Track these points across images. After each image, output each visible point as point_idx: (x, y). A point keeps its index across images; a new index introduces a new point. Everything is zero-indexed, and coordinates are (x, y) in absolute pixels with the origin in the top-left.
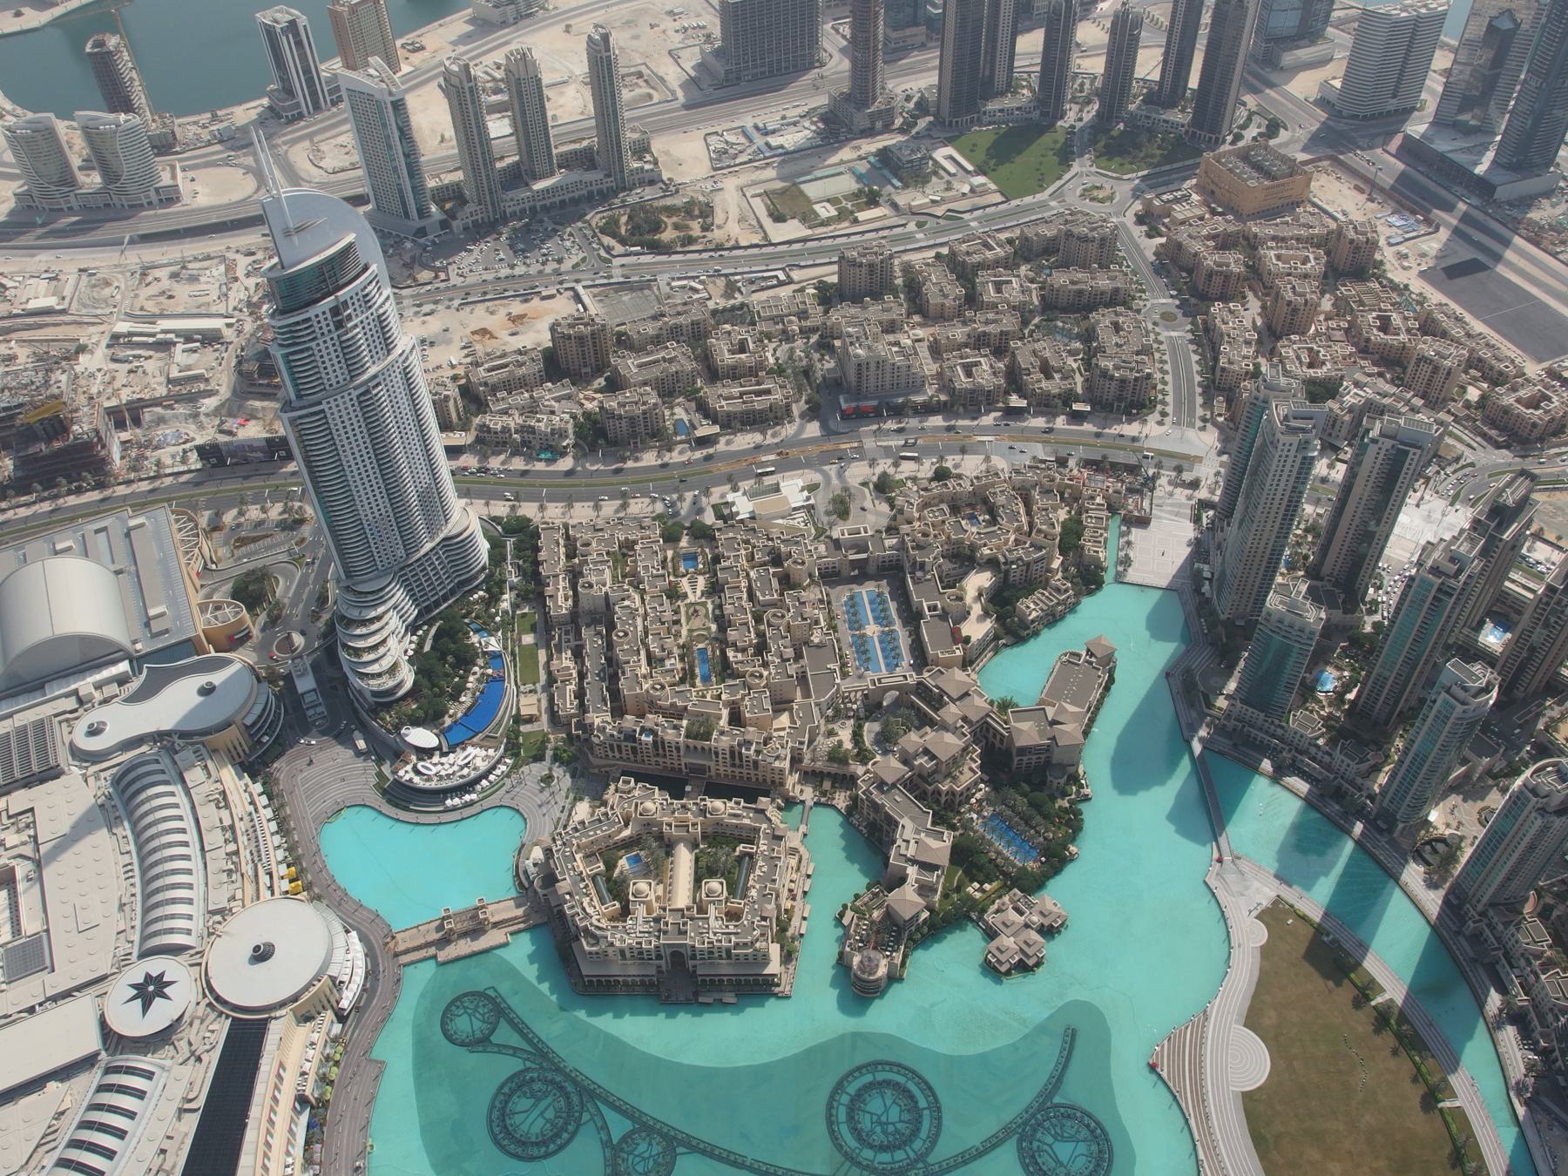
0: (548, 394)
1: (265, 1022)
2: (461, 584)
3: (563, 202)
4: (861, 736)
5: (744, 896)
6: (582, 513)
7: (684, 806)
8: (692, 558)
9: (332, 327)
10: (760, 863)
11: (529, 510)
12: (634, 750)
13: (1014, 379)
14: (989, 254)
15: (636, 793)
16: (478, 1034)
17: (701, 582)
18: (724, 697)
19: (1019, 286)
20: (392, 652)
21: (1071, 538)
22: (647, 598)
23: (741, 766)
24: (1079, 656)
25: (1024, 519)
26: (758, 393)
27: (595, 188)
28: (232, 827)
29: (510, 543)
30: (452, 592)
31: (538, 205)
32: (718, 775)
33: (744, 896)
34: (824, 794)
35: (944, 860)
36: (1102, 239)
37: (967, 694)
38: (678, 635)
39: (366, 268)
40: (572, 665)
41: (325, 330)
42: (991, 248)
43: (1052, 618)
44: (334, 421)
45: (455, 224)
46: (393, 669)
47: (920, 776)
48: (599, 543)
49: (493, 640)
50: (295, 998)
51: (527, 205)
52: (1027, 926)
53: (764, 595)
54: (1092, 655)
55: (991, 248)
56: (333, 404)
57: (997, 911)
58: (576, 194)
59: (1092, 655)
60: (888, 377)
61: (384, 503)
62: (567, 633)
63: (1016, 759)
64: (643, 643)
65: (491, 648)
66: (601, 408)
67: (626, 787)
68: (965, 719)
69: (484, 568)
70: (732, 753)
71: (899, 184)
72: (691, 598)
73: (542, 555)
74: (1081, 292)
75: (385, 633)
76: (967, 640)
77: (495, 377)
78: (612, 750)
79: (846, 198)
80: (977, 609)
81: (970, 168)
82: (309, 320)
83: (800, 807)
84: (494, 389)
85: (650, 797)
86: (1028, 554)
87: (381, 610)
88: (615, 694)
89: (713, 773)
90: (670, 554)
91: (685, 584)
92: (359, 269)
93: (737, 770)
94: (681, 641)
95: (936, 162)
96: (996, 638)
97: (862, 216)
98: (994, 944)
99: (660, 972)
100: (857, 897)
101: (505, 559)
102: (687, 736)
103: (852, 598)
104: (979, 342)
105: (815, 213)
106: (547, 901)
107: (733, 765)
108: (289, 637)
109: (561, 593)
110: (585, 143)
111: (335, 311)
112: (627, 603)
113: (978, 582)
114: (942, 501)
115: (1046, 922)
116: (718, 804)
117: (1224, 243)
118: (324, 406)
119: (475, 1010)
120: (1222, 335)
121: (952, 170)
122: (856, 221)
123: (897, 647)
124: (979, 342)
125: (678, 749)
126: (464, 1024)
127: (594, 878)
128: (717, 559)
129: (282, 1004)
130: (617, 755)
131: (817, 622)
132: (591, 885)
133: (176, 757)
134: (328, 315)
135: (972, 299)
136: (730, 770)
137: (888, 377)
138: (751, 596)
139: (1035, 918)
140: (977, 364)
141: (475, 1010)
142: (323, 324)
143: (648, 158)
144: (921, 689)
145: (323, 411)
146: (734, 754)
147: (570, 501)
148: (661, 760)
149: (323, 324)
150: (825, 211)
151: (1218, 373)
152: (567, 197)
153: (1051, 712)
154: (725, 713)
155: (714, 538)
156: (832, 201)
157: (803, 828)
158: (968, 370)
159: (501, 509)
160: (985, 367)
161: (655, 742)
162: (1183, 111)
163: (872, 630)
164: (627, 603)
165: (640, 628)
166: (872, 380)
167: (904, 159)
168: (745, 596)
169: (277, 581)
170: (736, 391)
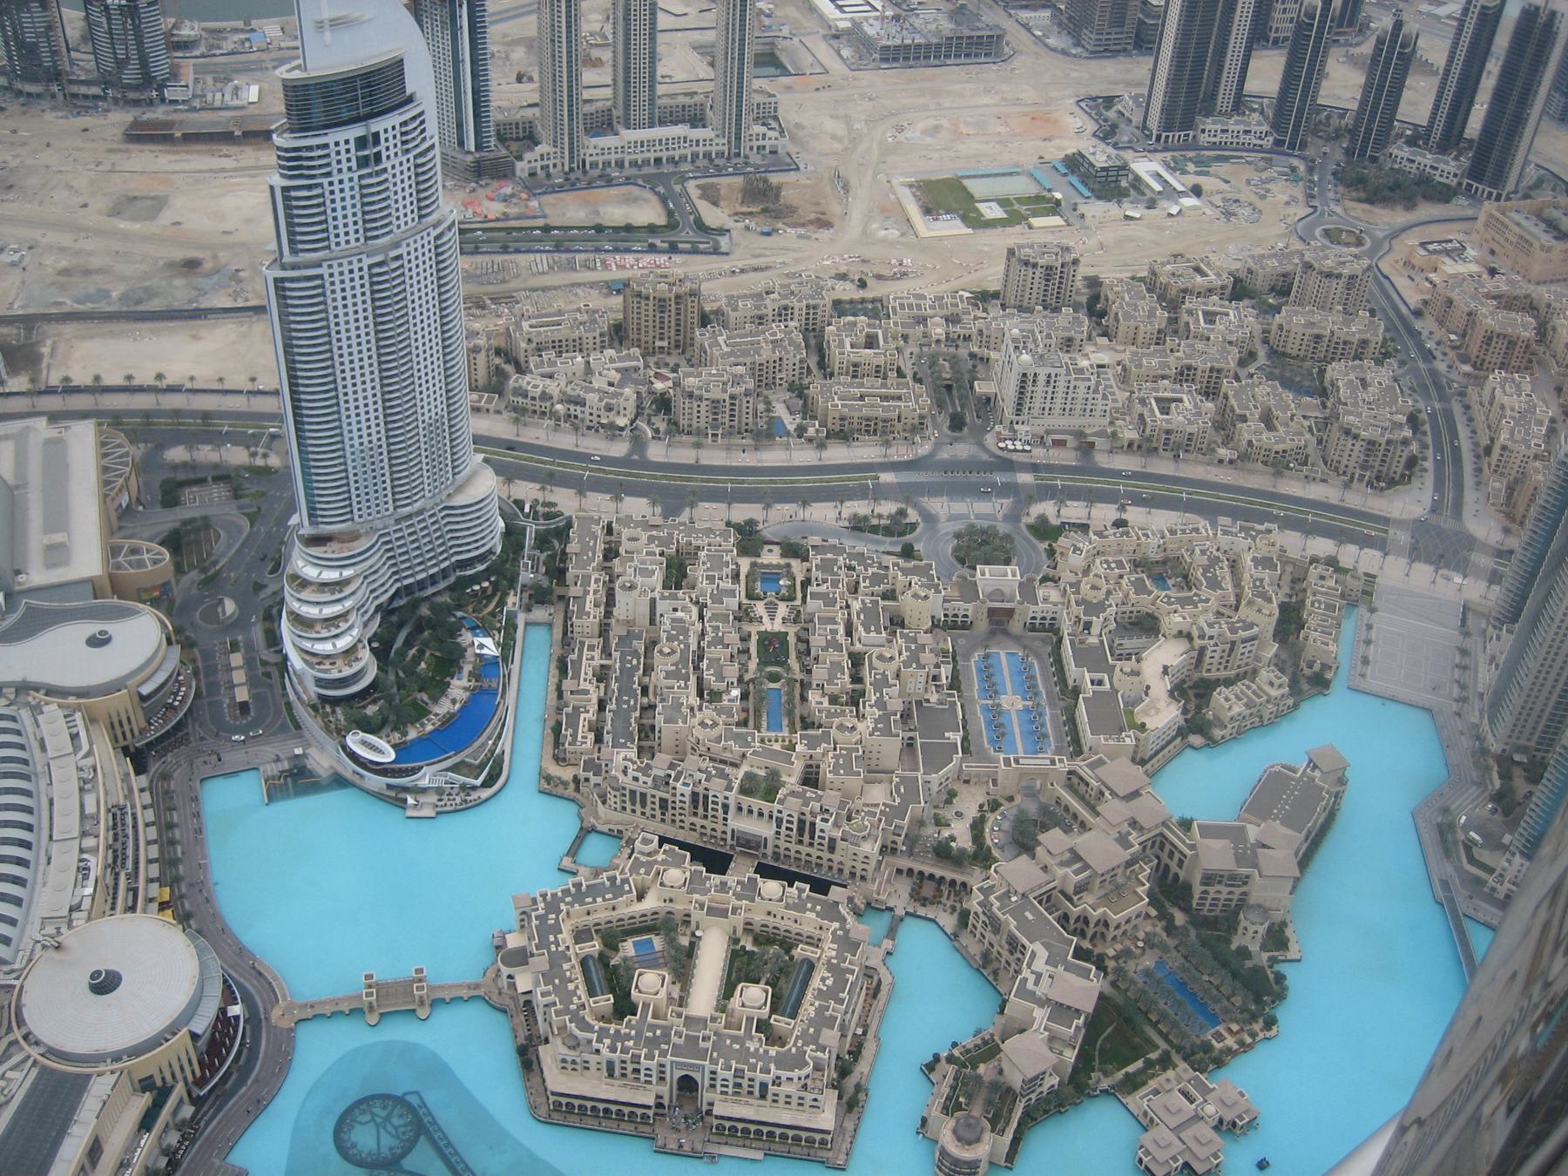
0: (608, 364)
1: (89, 1076)
2: (463, 565)
3: (658, 161)
4: (982, 831)
5: (793, 1016)
6: (637, 506)
7: (724, 884)
8: (770, 575)
9: (354, 164)
10: (820, 972)
11: (566, 501)
12: (664, 803)
13: (1225, 424)
14: (1199, 279)
15: (660, 857)
16: (385, 1151)
17: (783, 609)
18: (799, 748)
19: (1240, 320)
20: (355, 632)
21: (1290, 621)
22: (708, 614)
23: (811, 845)
24: (1294, 771)
25: (1228, 585)
26: (885, 398)
27: (701, 149)
28: (96, 817)
29: (531, 530)
30: (445, 573)
31: (627, 158)
32: (776, 856)
33: (793, 1016)
34: (924, 902)
35: (1089, 1006)
36: (1351, 277)
37: (1136, 794)
38: (744, 668)
39: (410, 100)
40: (592, 688)
41: (344, 166)
42: (1203, 274)
43: (1260, 721)
44: (335, 299)
45: (519, 165)
46: (350, 653)
47: (1062, 892)
48: (651, 539)
49: (488, 641)
50: (136, 1051)
51: (613, 157)
52: (1197, 1118)
53: (868, 631)
54: (1315, 767)
55: (1203, 274)
56: (336, 270)
57: (1156, 1092)
58: (677, 154)
59: (1315, 767)
60: (1060, 395)
61: (378, 433)
62: (591, 648)
63: (1197, 889)
64: (696, 668)
65: (485, 651)
66: (677, 384)
67: (647, 848)
68: (1134, 824)
69: (490, 552)
70: (801, 822)
71: (1087, 193)
72: (767, 626)
73: (573, 547)
74: (1318, 337)
75: (348, 604)
76: (1143, 727)
77: (547, 334)
78: (633, 803)
79: (1019, 200)
80: (1160, 688)
81: (1180, 188)
82: (326, 146)
83: (887, 916)
84: (539, 350)
85: (679, 864)
86: (1233, 630)
87: (347, 573)
88: (647, 731)
89: (769, 851)
90: (744, 570)
91: (760, 608)
92: (400, 99)
93: (804, 849)
94: (747, 677)
95: (1137, 178)
96: (1182, 732)
97: (1035, 221)
98: (1153, 1133)
99: (659, 1105)
100: (955, 1045)
101: (523, 547)
102: (743, 791)
103: (987, 656)
104: (1185, 374)
105: (977, 210)
106: (513, 986)
107: (801, 842)
108: (221, 601)
109: (590, 598)
110: (697, 99)
111: (361, 142)
112: (679, 614)
113: (1163, 656)
114: (1121, 552)
115: (1228, 1117)
116: (772, 887)
117: (1508, 303)
118: (324, 271)
119: (388, 1118)
120: (1503, 407)
121: (1158, 188)
122: (1030, 227)
123: (1043, 725)
124: (1185, 374)
125: (726, 807)
126: (365, 1138)
127: (584, 962)
128: (806, 583)
129: (117, 1057)
130: (638, 808)
131: (935, 678)
132: (578, 969)
133: (40, 718)
134: (352, 146)
135: (1174, 327)
136: (794, 847)
137: (1060, 395)
138: (849, 633)
139: (1210, 1109)
140: (1181, 400)
141: (388, 1118)
142: (343, 157)
143: (774, 124)
144: (1074, 781)
145: (321, 277)
146: (805, 828)
147: (618, 490)
148: (699, 821)
149: (343, 157)
150: (992, 211)
151: (1496, 451)
152: (664, 155)
153: (1253, 832)
154: (798, 766)
155: (805, 559)
156: (1004, 202)
157: (887, 944)
158: (1165, 405)
159: (526, 491)
160: (1187, 403)
161: (695, 795)
162: (1456, 158)
163: (1012, 702)
164: (679, 614)
165: (693, 647)
166: (1039, 395)
167: (1098, 165)
168: (842, 631)
169: (218, 537)
170: (857, 391)
